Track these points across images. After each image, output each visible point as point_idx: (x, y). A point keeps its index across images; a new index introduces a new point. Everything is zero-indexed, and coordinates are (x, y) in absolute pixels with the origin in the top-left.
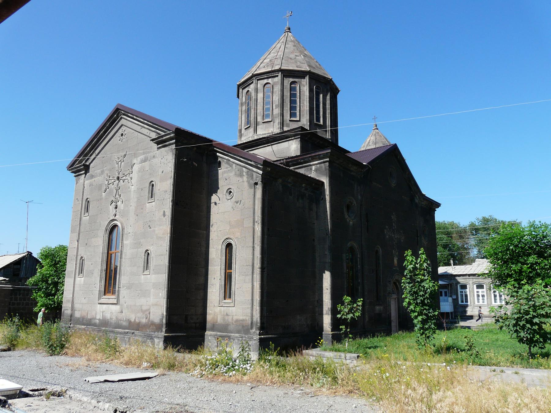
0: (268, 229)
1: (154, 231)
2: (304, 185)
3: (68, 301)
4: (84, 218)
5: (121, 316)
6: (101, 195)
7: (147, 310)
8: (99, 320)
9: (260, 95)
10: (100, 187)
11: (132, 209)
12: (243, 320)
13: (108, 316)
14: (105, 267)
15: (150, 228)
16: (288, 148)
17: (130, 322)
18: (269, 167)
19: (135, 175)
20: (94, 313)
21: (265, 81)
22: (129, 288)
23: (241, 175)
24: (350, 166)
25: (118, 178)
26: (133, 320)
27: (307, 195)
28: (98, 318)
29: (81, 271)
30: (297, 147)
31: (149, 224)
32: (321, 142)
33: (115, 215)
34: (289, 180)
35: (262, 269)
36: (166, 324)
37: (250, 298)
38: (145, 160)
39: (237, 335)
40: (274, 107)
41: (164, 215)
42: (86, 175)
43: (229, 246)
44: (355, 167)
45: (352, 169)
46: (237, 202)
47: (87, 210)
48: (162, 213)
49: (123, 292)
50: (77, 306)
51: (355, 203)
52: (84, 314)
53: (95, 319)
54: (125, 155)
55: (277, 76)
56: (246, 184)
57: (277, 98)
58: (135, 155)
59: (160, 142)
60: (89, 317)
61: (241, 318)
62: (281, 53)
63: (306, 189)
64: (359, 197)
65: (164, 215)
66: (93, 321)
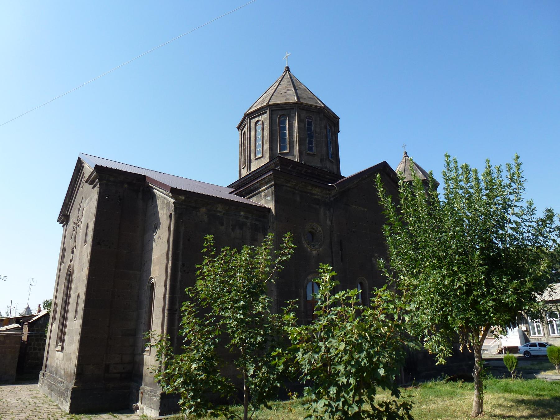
9: (253, 133)
21: (257, 119)
24: (309, 188)
27: (249, 224)
32: (309, 171)
34: (218, 209)
40: (264, 143)
44: (317, 189)
45: (314, 192)
51: (320, 229)
55: (266, 112)
62: (273, 91)
63: (247, 218)
64: (329, 223)
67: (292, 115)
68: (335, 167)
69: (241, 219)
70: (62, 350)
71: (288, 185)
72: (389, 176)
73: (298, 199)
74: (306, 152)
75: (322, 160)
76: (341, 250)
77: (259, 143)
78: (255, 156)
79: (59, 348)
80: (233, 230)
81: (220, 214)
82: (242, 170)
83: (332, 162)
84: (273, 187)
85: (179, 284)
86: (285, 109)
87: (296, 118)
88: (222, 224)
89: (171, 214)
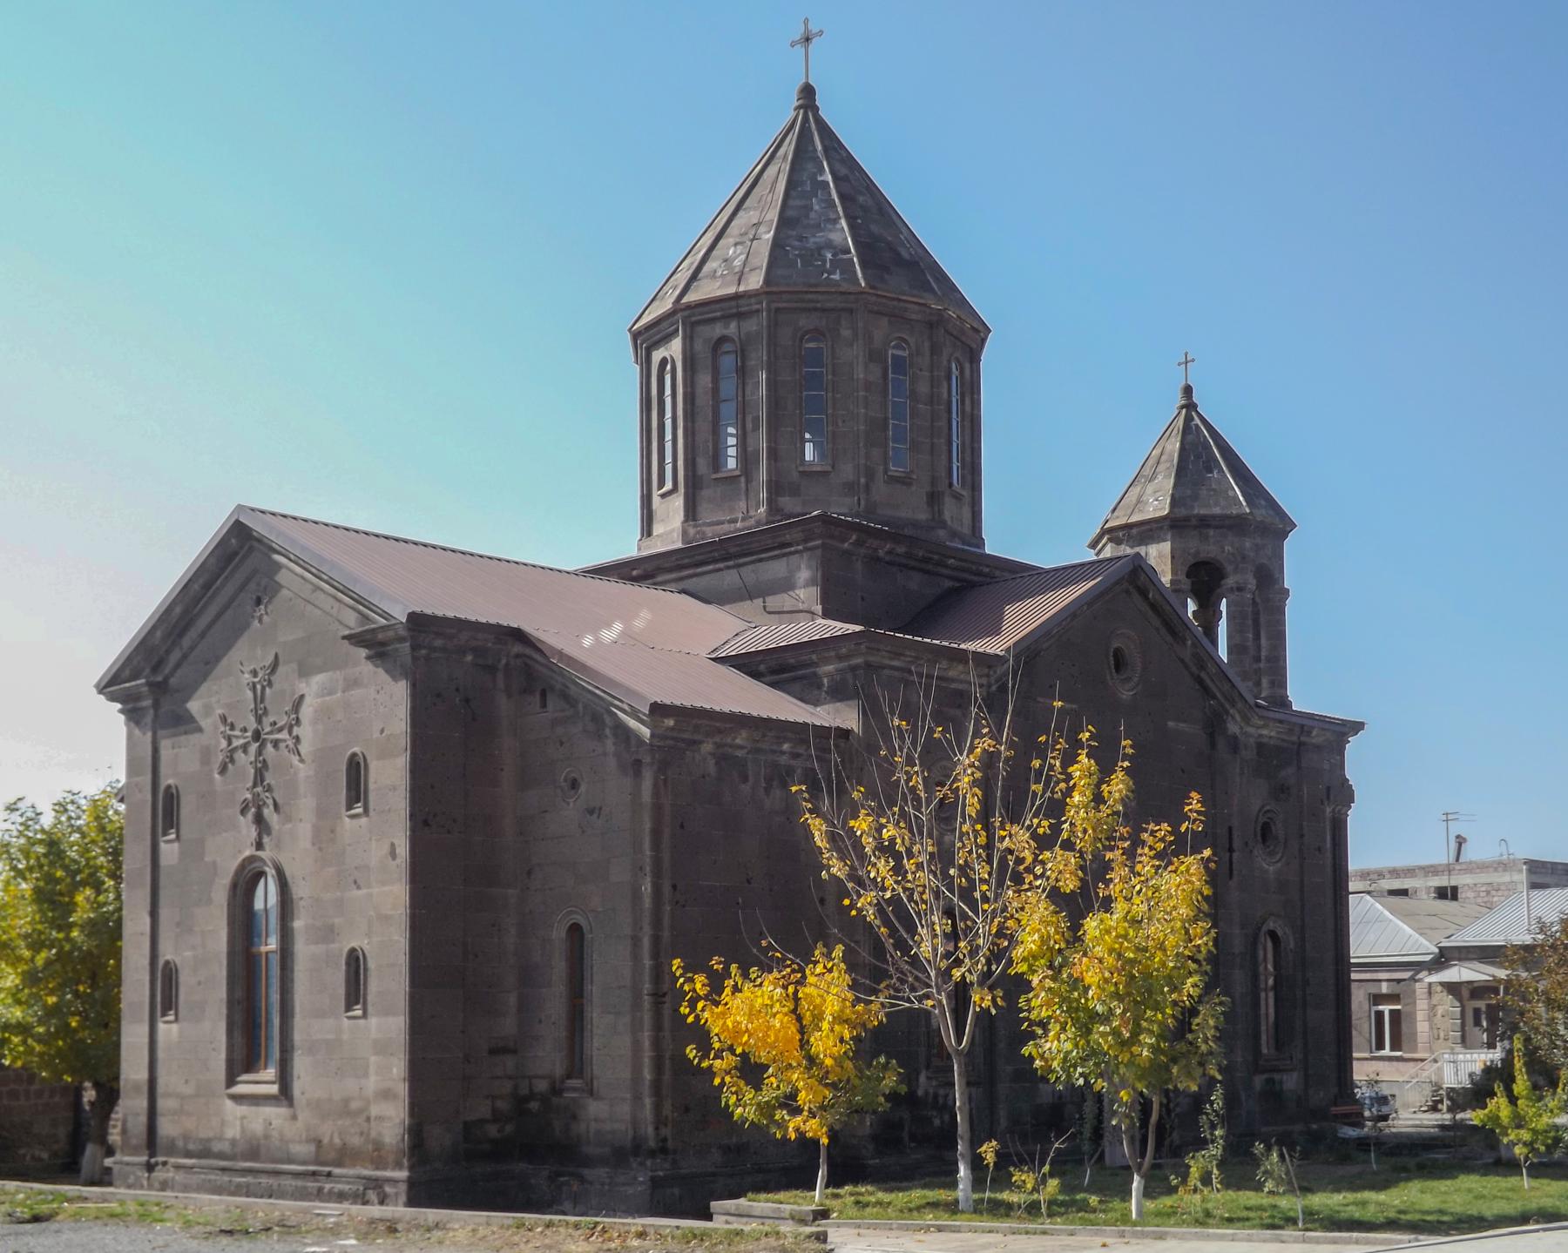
0: (674, 887)
2: (786, 747)
3: (136, 1088)
4: (163, 846)
6: (211, 780)
7: (360, 1111)
11: (305, 829)
14: (239, 994)
15: (359, 888)
17: (319, 1143)
18: (667, 716)
19: (305, 731)
22: (312, 1049)
23: (599, 736)
25: (257, 736)
32: (901, 549)
33: (259, 846)
34: (738, 741)
41: (393, 854)
43: (575, 930)
45: (951, 674)
46: (591, 812)
54: (274, 667)
56: (612, 762)
58: (305, 672)
59: (374, 644)
60: (202, 1135)
63: (796, 756)
65: (393, 854)
66: (217, 1147)
68: (966, 513)
69: (784, 760)
71: (896, 663)
72: (1143, 593)
74: (886, 472)
75: (934, 498)
79: (274, 1089)
80: (767, 790)
81: (739, 753)
82: (656, 500)
83: (957, 497)
88: (745, 779)
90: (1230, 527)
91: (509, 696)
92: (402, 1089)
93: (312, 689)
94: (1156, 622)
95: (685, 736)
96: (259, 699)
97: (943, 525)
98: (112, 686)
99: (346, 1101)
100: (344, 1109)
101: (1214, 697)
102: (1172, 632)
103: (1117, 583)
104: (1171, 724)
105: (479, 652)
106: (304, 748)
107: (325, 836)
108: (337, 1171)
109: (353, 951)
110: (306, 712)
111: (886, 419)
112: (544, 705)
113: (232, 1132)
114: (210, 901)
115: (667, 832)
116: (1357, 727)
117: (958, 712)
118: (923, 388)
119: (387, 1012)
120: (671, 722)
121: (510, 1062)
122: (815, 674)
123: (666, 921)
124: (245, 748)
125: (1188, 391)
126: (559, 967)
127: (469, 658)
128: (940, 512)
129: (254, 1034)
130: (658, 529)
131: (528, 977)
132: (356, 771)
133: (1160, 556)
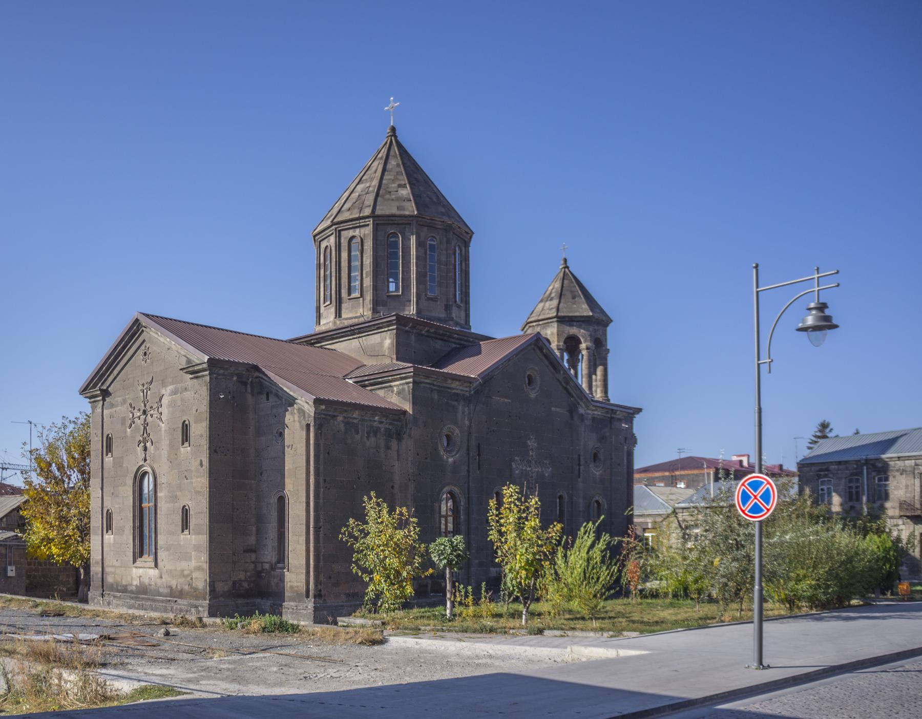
0: (325, 481)
1: (192, 483)
2: (376, 418)
3: (97, 563)
5: (159, 582)
6: (126, 432)
7: (188, 575)
8: (136, 586)
10: (123, 420)
11: (164, 453)
12: (297, 587)
13: (146, 581)
16: (381, 344)
17: (171, 588)
19: (164, 410)
20: (129, 578)
21: (351, 233)
22: (168, 548)
24: (450, 381)
26: (174, 587)
28: (135, 583)
29: (109, 527)
30: (392, 343)
31: (186, 473)
32: (432, 330)
35: (317, 529)
36: (210, 592)
37: (304, 562)
38: (174, 393)
39: (292, 604)
40: (364, 275)
41: (201, 465)
42: (104, 400)
44: (457, 383)
45: (453, 386)
47: (109, 449)
48: (198, 462)
49: (162, 554)
50: (107, 570)
51: (457, 431)
52: (118, 578)
53: (131, 585)
56: (297, 424)
57: (368, 260)
58: (164, 384)
60: (124, 583)
61: (295, 584)
63: (381, 422)
64: (467, 422)
65: (201, 465)
66: (129, 588)
67: (407, 234)
68: (463, 314)
69: (375, 424)
70: (156, 566)
72: (541, 349)
73: (436, 397)
75: (447, 307)
76: (479, 455)
77: (356, 274)
78: (349, 294)
79: (153, 565)
80: (368, 438)
81: (355, 421)
83: (459, 307)
84: (411, 385)
85: (321, 501)
86: (398, 224)
87: (413, 239)
88: (357, 433)
89: (308, 426)
90: (583, 321)
91: (253, 395)
92: (206, 566)
93: (166, 391)
94: (547, 363)
95: (331, 413)
96: (145, 397)
97: (452, 319)
98: (84, 391)
99: (183, 571)
100: (182, 574)
101: (573, 397)
102: (554, 367)
103: (530, 345)
104: (553, 409)
105: (239, 376)
106: (164, 418)
107: (173, 458)
108: (179, 601)
109: (184, 506)
110: (165, 401)
111: (426, 273)
112: (268, 399)
113: (136, 582)
114: (125, 485)
115: (322, 456)
116: (639, 410)
117: (456, 403)
118: (443, 258)
119: (198, 533)
120: (323, 407)
121: (253, 556)
122: (391, 386)
123: (321, 495)
124: (139, 418)
125: (565, 260)
126: (274, 514)
127: (235, 378)
128: (451, 313)
129: (143, 543)
130: (323, 322)
131: (260, 519)
132: (185, 428)
133: (552, 334)
